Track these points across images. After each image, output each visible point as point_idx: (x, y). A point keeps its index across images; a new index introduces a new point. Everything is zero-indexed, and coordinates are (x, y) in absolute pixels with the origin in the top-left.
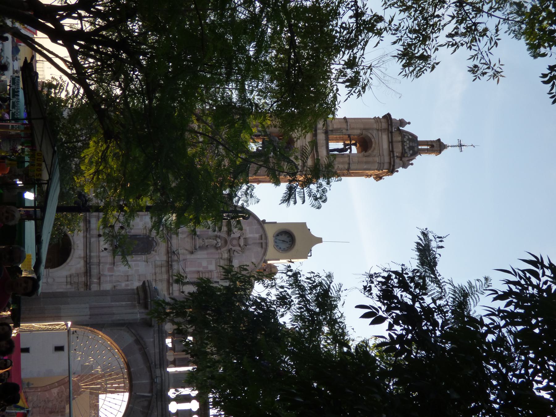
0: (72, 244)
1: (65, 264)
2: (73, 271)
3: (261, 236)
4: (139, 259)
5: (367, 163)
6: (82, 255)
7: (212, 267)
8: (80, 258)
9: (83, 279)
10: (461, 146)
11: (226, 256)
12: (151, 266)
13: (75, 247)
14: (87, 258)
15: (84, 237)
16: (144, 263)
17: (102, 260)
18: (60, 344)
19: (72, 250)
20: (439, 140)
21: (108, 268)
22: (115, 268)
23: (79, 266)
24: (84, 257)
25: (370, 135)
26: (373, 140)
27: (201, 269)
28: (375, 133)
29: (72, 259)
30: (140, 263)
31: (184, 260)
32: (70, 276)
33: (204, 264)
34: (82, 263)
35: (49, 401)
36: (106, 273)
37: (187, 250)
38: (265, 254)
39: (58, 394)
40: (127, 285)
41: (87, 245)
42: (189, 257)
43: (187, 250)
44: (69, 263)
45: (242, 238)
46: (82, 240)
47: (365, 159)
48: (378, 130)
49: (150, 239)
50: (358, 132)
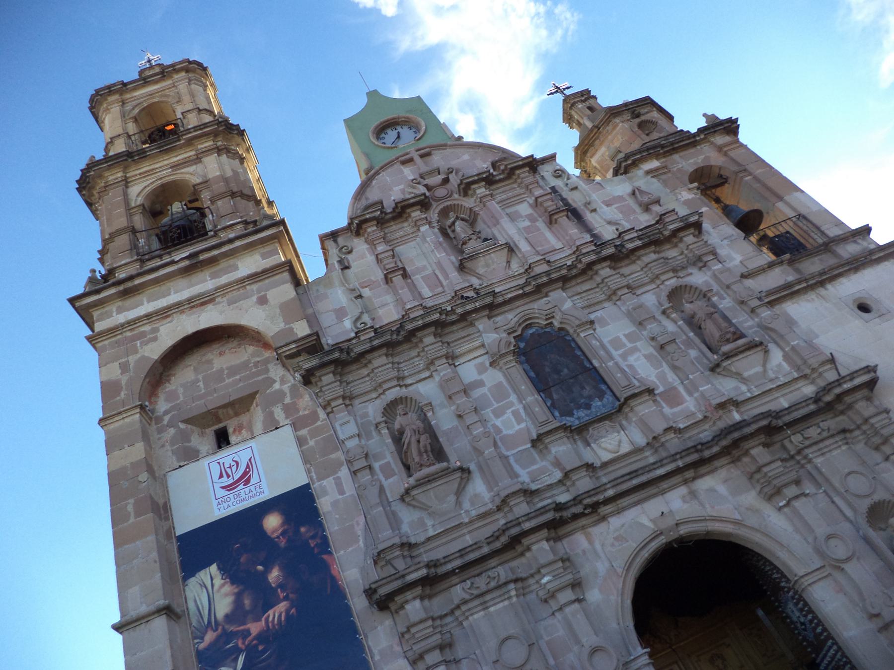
0: (662, 540)
2: (750, 498)
3: (404, 163)
6: (683, 490)
7: (524, 209)
8: (693, 494)
9: (759, 453)
11: (481, 191)
12: (598, 314)
13: (670, 522)
14: (687, 467)
15: (619, 511)
16: (599, 330)
17: (659, 427)
19: (683, 530)
22: (661, 389)
23: (722, 489)
24: (686, 482)
25: (137, 111)
27: (541, 224)
30: (605, 341)
34: (705, 483)
36: (690, 404)
37: (508, 262)
38: (442, 146)
40: (689, 343)
41: (642, 486)
42: (524, 246)
43: (508, 262)
44: (736, 523)
45: (425, 182)
46: (631, 515)
49: (522, 345)
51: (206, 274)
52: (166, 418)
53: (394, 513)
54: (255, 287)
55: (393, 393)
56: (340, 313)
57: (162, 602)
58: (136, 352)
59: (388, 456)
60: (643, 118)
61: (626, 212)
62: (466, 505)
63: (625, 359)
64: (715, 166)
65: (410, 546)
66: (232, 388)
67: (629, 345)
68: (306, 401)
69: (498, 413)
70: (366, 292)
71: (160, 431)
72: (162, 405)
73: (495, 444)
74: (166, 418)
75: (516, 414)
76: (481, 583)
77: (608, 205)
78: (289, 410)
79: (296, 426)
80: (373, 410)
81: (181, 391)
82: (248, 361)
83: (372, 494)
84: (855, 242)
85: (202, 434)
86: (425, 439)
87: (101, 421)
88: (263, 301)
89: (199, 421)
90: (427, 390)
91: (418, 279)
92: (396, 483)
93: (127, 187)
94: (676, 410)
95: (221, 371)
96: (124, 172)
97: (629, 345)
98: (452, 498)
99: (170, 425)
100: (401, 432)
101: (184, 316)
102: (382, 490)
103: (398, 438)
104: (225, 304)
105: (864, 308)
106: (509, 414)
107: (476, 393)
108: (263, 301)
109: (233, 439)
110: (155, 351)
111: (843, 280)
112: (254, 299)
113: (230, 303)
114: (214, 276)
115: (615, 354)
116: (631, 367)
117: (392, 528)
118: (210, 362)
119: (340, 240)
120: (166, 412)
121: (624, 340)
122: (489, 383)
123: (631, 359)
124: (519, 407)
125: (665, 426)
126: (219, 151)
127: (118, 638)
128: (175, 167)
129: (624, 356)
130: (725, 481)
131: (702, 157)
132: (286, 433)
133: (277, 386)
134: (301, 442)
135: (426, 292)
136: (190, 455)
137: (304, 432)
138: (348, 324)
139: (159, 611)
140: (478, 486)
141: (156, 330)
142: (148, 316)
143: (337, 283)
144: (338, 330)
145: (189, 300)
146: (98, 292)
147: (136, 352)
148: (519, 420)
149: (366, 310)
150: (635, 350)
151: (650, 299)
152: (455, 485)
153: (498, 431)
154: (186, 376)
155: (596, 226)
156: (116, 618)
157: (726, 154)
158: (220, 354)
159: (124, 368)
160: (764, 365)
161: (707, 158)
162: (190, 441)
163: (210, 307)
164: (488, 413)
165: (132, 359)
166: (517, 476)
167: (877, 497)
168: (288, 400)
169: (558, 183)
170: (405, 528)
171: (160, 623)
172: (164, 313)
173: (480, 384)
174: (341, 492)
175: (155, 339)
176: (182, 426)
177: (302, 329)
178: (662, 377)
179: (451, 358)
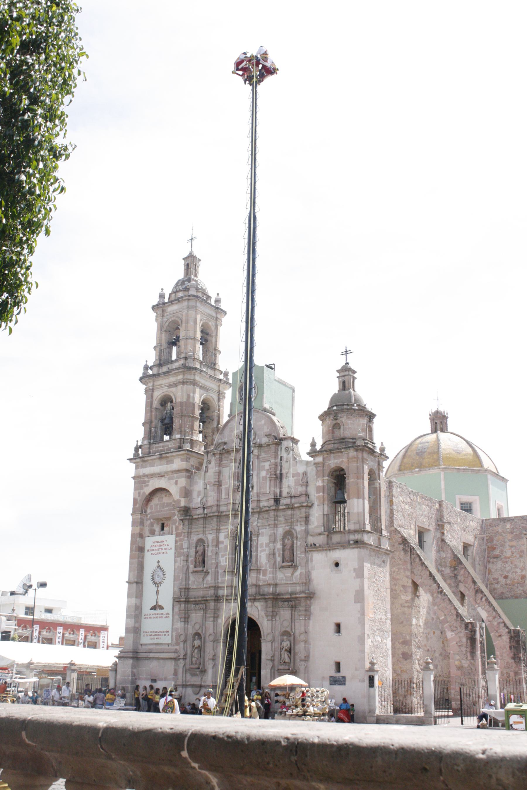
1: (257, 622)
4: (254, 543)
5: (187, 322)
7: (267, 465)
10: (192, 239)
12: (263, 530)
16: (260, 538)
18: (333, 627)
20: (184, 259)
21: (263, 576)
22: (264, 569)
25: (167, 324)
26: (171, 320)
28: (165, 319)
29: (253, 615)
30: (259, 543)
31: (258, 496)
32: (267, 616)
33: (263, 474)
35: (460, 641)
39: (452, 631)
47: (184, 325)
48: (163, 316)
50: (164, 335)
51: (164, 461)
52: (149, 516)
53: (189, 576)
54: (175, 475)
55: (201, 536)
56: (199, 492)
57: (136, 580)
58: (143, 489)
59: (191, 559)
60: (338, 421)
61: (296, 483)
62: (205, 582)
63: (260, 553)
64: (127, 624)
65: (188, 589)
66: (165, 512)
67: (264, 548)
68: (181, 527)
69: (223, 556)
70: (208, 486)
71: (147, 520)
72: (149, 511)
73: (217, 567)
74: (149, 516)
75: (226, 558)
76: (197, 606)
77: (293, 477)
78: (177, 528)
79: (177, 536)
80: (195, 538)
81: (154, 506)
82: (171, 503)
83: (185, 569)
84: (354, 534)
85: (158, 523)
86: (201, 558)
87: (132, 514)
88: (176, 483)
89: (158, 520)
90: (210, 537)
91: (223, 487)
92: (191, 567)
93: (153, 391)
94: (264, 577)
95: (164, 503)
96: (154, 382)
97: (264, 548)
98: (201, 579)
99: (149, 519)
100: (198, 552)
101: (156, 479)
102: (188, 568)
103: (196, 552)
104: (167, 479)
105: (337, 565)
106: (224, 558)
107: (221, 546)
108: (176, 483)
109: (165, 529)
110: (148, 490)
111: (338, 551)
112: (174, 481)
113: (169, 479)
114: (167, 464)
115: (259, 549)
116: (260, 556)
117: (186, 582)
118: (162, 498)
119: (209, 455)
120: (149, 513)
121: (264, 545)
122: (225, 544)
123: (262, 553)
124: (228, 557)
125: (254, 582)
126: (183, 383)
127: (127, 584)
128: (170, 386)
129: (261, 551)
130: (262, 606)
131: (341, 460)
132: (174, 536)
133: (176, 517)
134: (176, 542)
135: (223, 497)
136: (152, 533)
137: (178, 539)
138: (199, 499)
139: (135, 582)
140: (209, 578)
141: (148, 481)
142: (147, 476)
143: (202, 477)
144: (196, 501)
145: (158, 474)
146: (135, 459)
147: (143, 489)
148: (226, 562)
149: (206, 496)
150: (265, 550)
151: (280, 531)
152: (203, 576)
153: (220, 562)
154: (155, 501)
155: (284, 486)
156: (127, 580)
157: (349, 464)
158: (166, 496)
159: (139, 493)
160: (292, 574)
161: (342, 461)
162: (153, 526)
163: (163, 478)
164: (220, 554)
165: (142, 491)
166: (218, 579)
167: (287, 629)
168: (177, 524)
169: (284, 454)
170: (190, 582)
171: (135, 585)
172: (151, 476)
173: (222, 542)
174: (180, 564)
175: (148, 486)
176: (152, 521)
177: (183, 503)
178: (266, 564)
179: (218, 530)
